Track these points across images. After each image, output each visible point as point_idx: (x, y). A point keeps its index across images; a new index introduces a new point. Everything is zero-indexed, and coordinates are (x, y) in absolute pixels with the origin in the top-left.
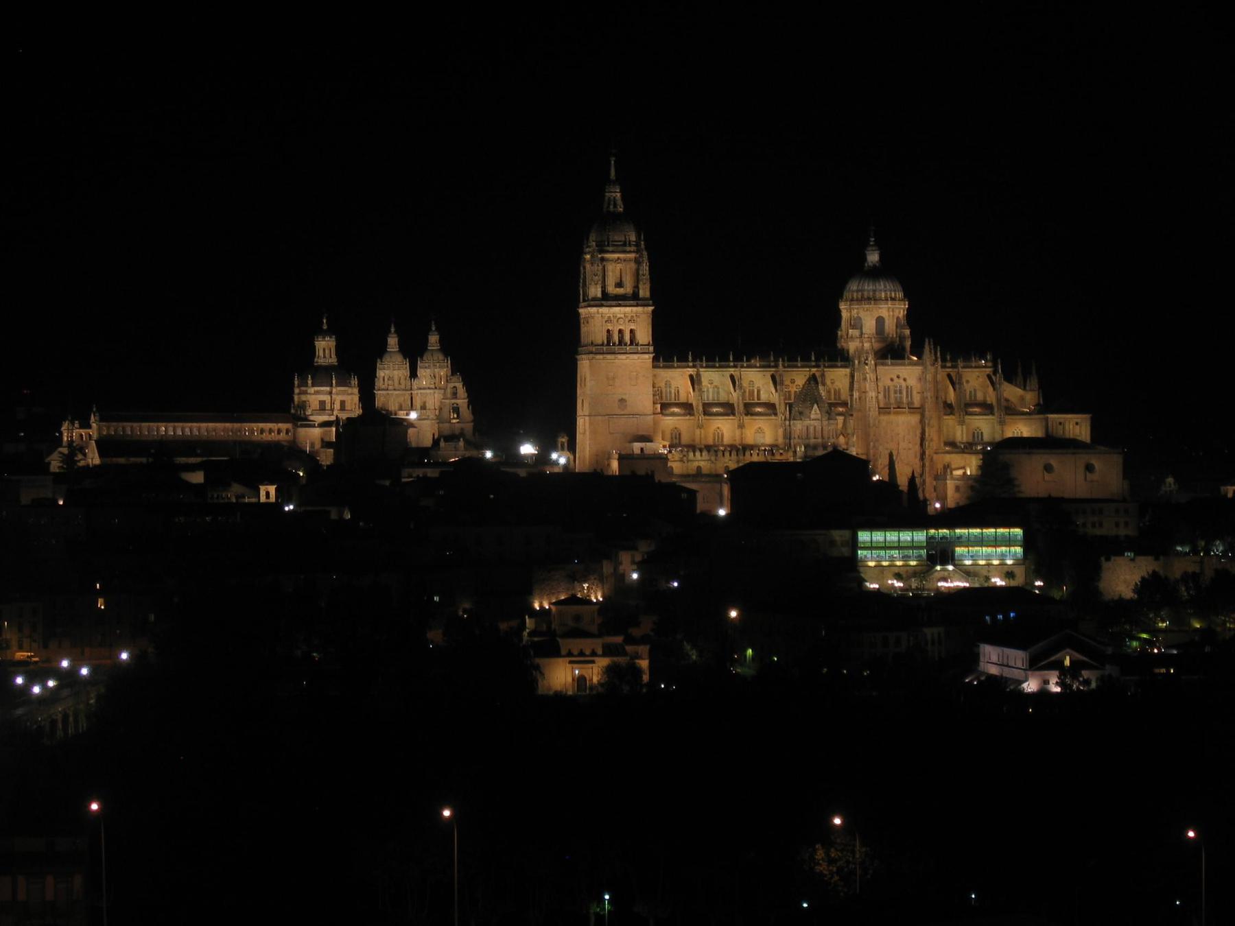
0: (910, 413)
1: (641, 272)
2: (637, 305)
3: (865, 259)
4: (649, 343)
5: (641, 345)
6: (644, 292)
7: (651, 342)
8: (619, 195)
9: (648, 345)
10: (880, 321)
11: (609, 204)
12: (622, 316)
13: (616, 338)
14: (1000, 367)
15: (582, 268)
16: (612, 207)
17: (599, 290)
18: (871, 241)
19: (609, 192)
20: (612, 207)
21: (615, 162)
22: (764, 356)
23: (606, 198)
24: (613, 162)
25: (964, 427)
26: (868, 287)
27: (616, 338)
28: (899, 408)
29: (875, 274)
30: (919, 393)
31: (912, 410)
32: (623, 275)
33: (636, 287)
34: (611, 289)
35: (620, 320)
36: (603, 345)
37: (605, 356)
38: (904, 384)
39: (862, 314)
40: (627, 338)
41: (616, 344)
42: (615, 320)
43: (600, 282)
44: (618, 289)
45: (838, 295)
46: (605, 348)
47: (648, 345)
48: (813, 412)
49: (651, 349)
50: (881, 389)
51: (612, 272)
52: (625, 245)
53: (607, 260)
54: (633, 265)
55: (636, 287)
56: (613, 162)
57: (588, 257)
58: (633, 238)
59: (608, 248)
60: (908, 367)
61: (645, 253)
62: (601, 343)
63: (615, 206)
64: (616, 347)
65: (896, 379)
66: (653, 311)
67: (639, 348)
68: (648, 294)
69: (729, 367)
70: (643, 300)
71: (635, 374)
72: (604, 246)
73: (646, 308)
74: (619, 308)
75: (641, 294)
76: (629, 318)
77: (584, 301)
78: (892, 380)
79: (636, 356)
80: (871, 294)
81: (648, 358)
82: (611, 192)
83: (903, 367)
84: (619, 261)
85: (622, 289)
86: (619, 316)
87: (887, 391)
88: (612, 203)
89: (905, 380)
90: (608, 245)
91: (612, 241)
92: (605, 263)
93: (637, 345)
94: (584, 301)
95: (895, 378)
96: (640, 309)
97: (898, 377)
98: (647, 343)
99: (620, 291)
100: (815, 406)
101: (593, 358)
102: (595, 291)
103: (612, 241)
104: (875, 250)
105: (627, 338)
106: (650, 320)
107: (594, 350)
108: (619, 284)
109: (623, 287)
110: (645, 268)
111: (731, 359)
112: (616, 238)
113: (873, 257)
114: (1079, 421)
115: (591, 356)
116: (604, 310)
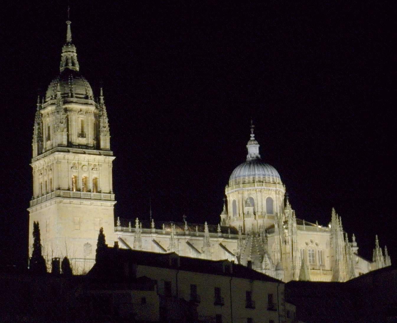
1: (102, 125)
2: (100, 155)
3: (246, 152)
4: (110, 191)
5: (104, 193)
6: (105, 142)
7: (112, 190)
8: (76, 55)
9: (110, 193)
10: (270, 201)
11: (67, 64)
12: (86, 163)
14: (377, 241)
15: (36, 127)
16: (70, 65)
17: (65, 137)
18: (251, 137)
19: (66, 52)
20: (70, 65)
21: (71, 25)
22: (179, 223)
23: (63, 59)
24: (69, 26)
26: (259, 172)
28: (313, 269)
29: (259, 162)
30: (328, 257)
31: (325, 272)
32: (85, 126)
33: (97, 138)
34: (76, 140)
35: (84, 167)
36: (69, 190)
37: (72, 200)
39: (253, 196)
40: (91, 186)
42: (80, 166)
43: (66, 130)
44: (80, 139)
45: (225, 182)
46: (71, 192)
47: (110, 193)
49: (113, 196)
51: (76, 122)
52: (87, 97)
53: (71, 111)
54: (92, 118)
55: (97, 138)
56: (69, 26)
57: (50, 109)
58: (91, 93)
59: (72, 99)
60: (319, 233)
61: (104, 107)
62: (67, 188)
63: (73, 64)
64: (82, 193)
65: (310, 245)
66: (114, 162)
67: (102, 194)
68: (108, 146)
69: (151, 233)
70: (104, 150)
71: (99, 219)
72: (68, 97)
73: (107, 157)
74: (84, 155)
75: (102, 145)
76: (92, 167)
77: (39, 154)
78: (307, 244)
79: (99, 203)
80: (262, 177)
81: (110, 206)
82: (69, 51)
83: (315, 233)
84: (81, 112)
85: (85, 139)
86: (83, 163)
87: (303, 252)
88: (70, 61)
89: (317, 245)
90: (72, 96)
91: (76, 94)
92: (68, 113)
93: (100, 192)
94: (39, 154)
96: (102, 158)
97: (312, 242)
98: (108, 192)
99: (82, 141)
101: (60, 202)
103: (76, 94)
104: (257, 144)
105: (91, 186)
106: (111, 169)
107: (62, 194)
108: (82, 135)
109: (85, 137)
110: (105, 121)
112: (79, 91)
115: (59, 199)
116: (70, 156)
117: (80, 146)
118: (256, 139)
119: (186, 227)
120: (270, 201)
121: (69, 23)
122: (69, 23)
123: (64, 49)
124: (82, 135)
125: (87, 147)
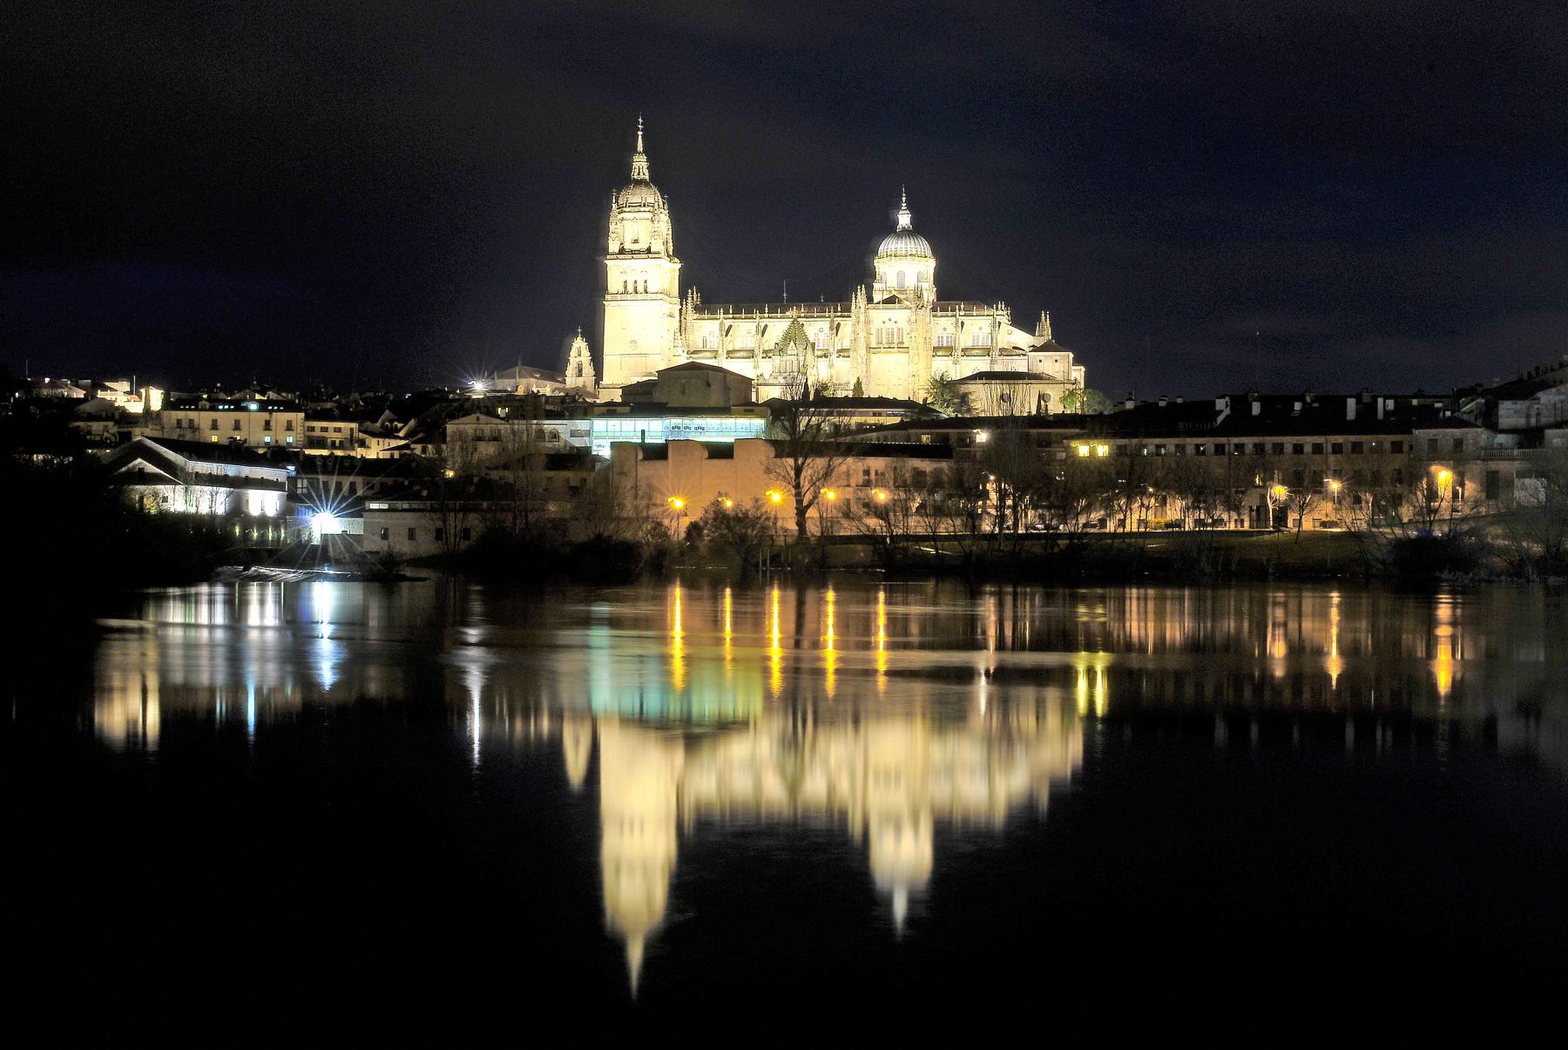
0: (899, 352)
10: (901, 275)
13: (630, 288)
24: (640, 137)
25: (958, 366)
27: (630, 288)
29: (906, 233)
34: (628, 246)
38: (895, 326)
40: (640, 289)
41: (634, 291)
48: (790, 348)
50: (873, 331)
56: (640, 137)
87: (879, 331)
95: (893, 321)
99: (635, 247)
100: (792, 343)
102: (613, 246)
111: (767, 311)
113: (904, 219)
114: (1057, 358)
117: (632, 252)
118: (909, 207)
119: (803, 310)
120: (901, 275)
121: (640, 133)
122: (640, 133)
123: (636, 158)
124: (636, 241)
125: (639, 252)
